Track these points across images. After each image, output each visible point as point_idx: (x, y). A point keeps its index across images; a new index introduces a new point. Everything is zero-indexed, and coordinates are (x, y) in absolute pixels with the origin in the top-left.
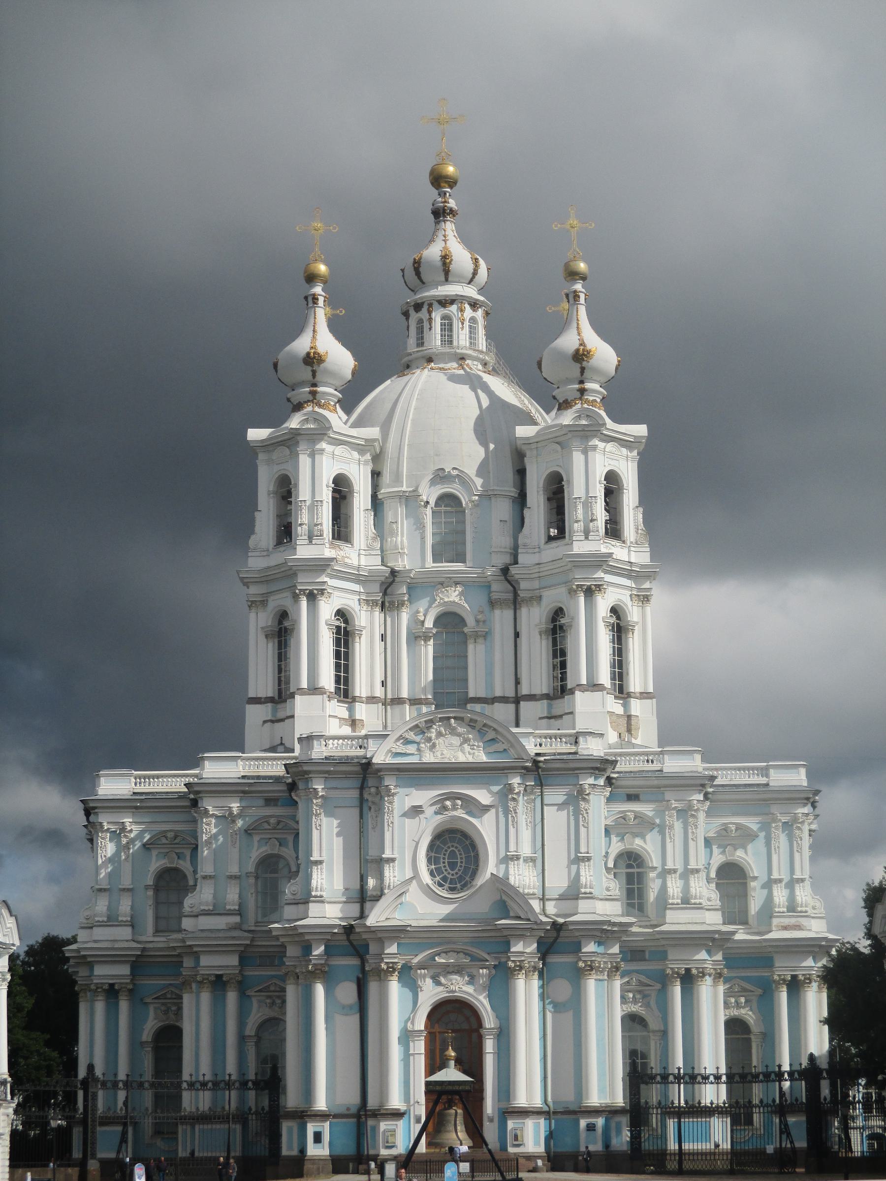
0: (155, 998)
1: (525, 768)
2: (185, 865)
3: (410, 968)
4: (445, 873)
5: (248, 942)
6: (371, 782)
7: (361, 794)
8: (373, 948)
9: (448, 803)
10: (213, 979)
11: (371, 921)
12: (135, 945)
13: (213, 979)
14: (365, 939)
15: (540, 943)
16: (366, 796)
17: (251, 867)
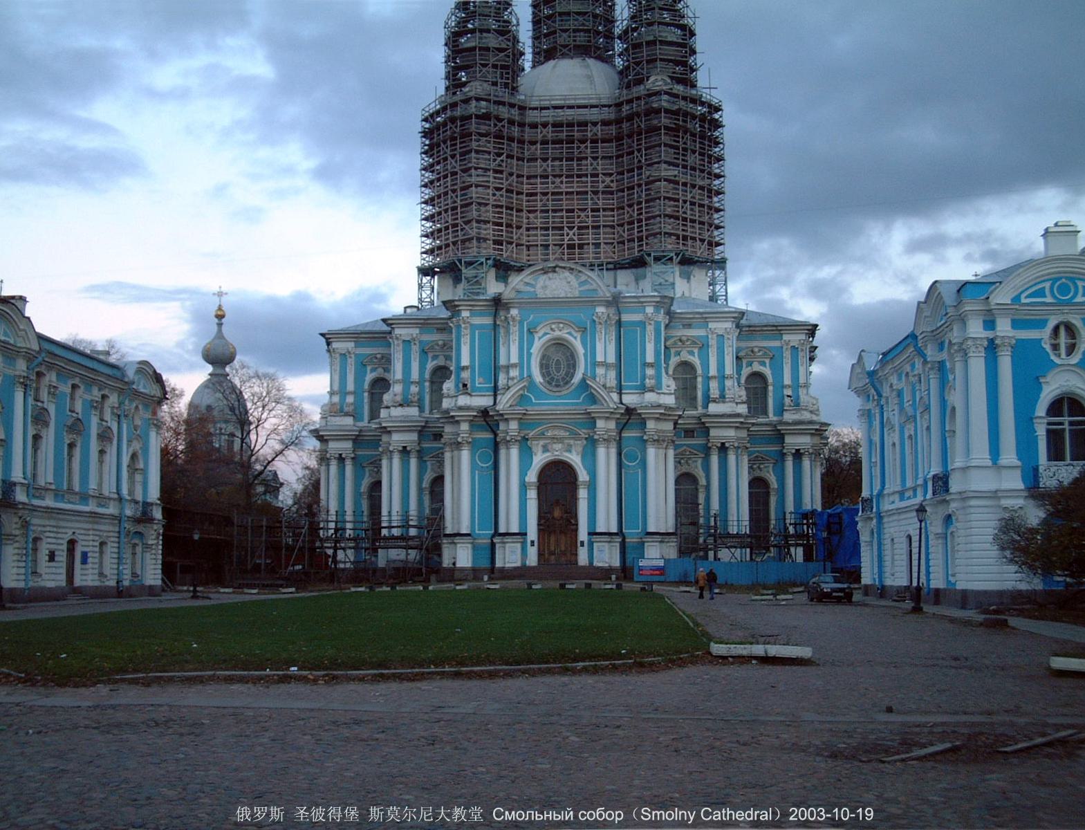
0: (371, 463)
1: (607, 301)
2: (386, 376)
3: (527, 439)
4: (553, 375)
5: (423, 424)
6: (502, 313)
7: (495, 321)
8: (502, 426)
9: (553, 326)
10: (401, 449)
11: (499, 407)
12: (355, 428)
13: (401, 449)
14: (496, 420)
15: (617, 424)
16: (498, 323)
17: (427, 376)
